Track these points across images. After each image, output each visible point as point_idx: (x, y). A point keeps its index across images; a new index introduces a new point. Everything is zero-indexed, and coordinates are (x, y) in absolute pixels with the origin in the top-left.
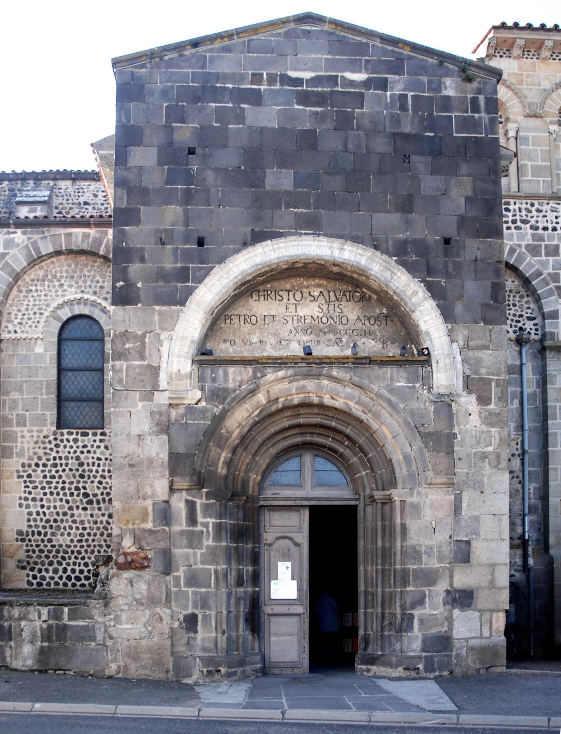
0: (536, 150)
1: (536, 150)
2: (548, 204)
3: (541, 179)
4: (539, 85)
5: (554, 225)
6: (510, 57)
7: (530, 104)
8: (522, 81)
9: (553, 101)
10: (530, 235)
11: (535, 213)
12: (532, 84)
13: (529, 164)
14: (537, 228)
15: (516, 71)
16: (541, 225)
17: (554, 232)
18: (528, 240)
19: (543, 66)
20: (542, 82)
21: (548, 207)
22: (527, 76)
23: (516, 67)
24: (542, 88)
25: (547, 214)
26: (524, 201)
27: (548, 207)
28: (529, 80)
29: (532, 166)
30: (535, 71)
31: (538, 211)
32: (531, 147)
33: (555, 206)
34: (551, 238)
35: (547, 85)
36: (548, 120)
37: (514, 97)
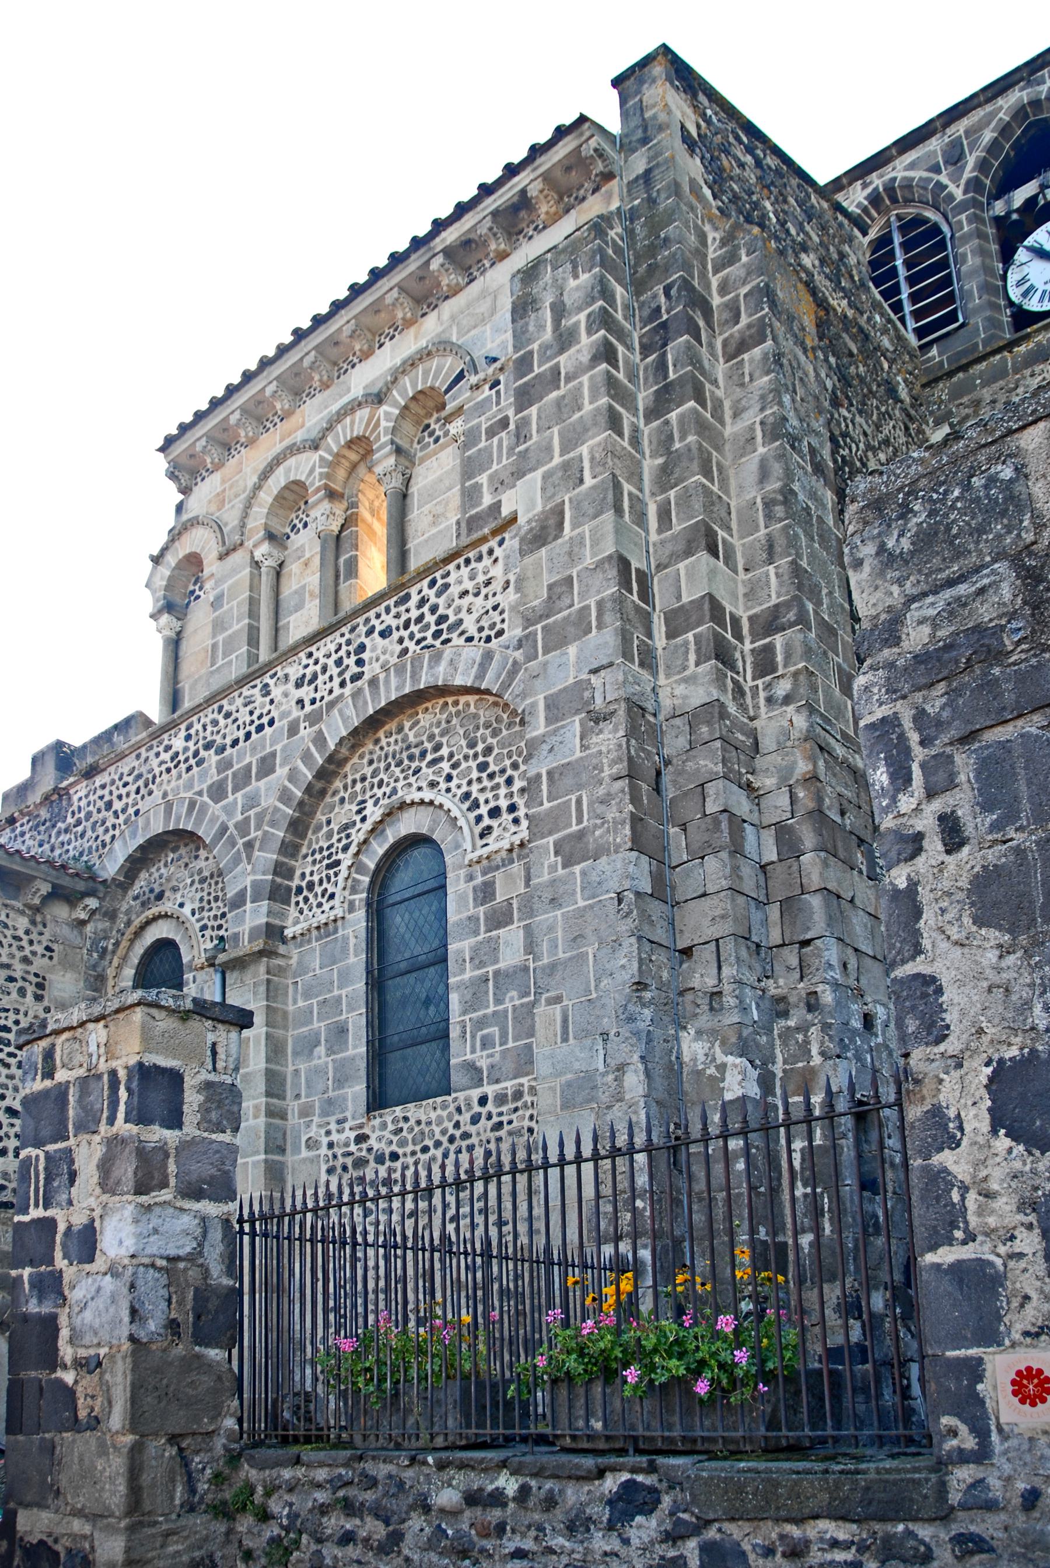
5: (248, 728)
10: (214, 765)
11: (222, 722)
14: (222, 749)
16: (228, 741)
18: (213, 777)
25: (238, 715)
26: (210, 709)
31: (228, 715)
34: (241, 756)
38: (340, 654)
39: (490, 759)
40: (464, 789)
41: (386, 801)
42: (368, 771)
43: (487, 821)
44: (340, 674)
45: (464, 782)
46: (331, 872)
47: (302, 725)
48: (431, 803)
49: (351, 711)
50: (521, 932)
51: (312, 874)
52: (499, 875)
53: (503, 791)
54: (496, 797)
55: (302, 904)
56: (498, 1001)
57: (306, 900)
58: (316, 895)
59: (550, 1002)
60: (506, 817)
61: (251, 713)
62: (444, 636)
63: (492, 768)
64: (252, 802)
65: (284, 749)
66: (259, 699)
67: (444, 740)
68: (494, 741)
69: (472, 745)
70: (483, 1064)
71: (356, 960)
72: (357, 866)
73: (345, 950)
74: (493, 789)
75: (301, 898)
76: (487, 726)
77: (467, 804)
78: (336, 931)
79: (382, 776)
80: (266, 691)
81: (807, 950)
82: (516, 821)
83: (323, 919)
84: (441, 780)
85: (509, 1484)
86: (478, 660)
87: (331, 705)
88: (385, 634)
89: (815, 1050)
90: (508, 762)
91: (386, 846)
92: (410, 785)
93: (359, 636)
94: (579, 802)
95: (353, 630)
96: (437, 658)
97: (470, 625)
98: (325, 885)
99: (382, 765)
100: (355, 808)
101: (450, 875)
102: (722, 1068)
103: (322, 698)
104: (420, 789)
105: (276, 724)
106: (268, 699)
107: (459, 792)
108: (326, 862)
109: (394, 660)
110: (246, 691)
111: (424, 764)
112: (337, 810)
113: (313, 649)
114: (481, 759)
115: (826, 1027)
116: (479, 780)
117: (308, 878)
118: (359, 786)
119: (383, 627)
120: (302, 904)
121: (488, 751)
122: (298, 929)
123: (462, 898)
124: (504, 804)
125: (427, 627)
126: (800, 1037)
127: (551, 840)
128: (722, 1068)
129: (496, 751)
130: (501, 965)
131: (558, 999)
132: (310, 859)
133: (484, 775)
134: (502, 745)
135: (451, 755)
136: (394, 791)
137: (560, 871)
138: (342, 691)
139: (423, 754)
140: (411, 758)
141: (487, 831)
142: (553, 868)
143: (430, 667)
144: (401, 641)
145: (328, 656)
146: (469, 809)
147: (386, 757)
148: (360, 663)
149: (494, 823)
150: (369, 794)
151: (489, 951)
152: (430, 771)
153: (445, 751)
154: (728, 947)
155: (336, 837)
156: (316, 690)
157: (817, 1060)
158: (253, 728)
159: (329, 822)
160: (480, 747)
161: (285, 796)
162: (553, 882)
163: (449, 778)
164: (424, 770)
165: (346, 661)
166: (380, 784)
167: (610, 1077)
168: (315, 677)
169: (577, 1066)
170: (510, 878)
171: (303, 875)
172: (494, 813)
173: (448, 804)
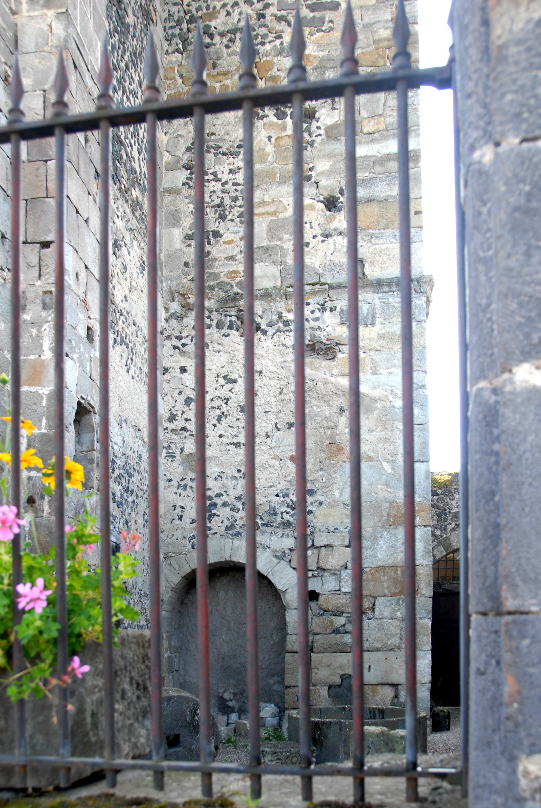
126: (34, 331)
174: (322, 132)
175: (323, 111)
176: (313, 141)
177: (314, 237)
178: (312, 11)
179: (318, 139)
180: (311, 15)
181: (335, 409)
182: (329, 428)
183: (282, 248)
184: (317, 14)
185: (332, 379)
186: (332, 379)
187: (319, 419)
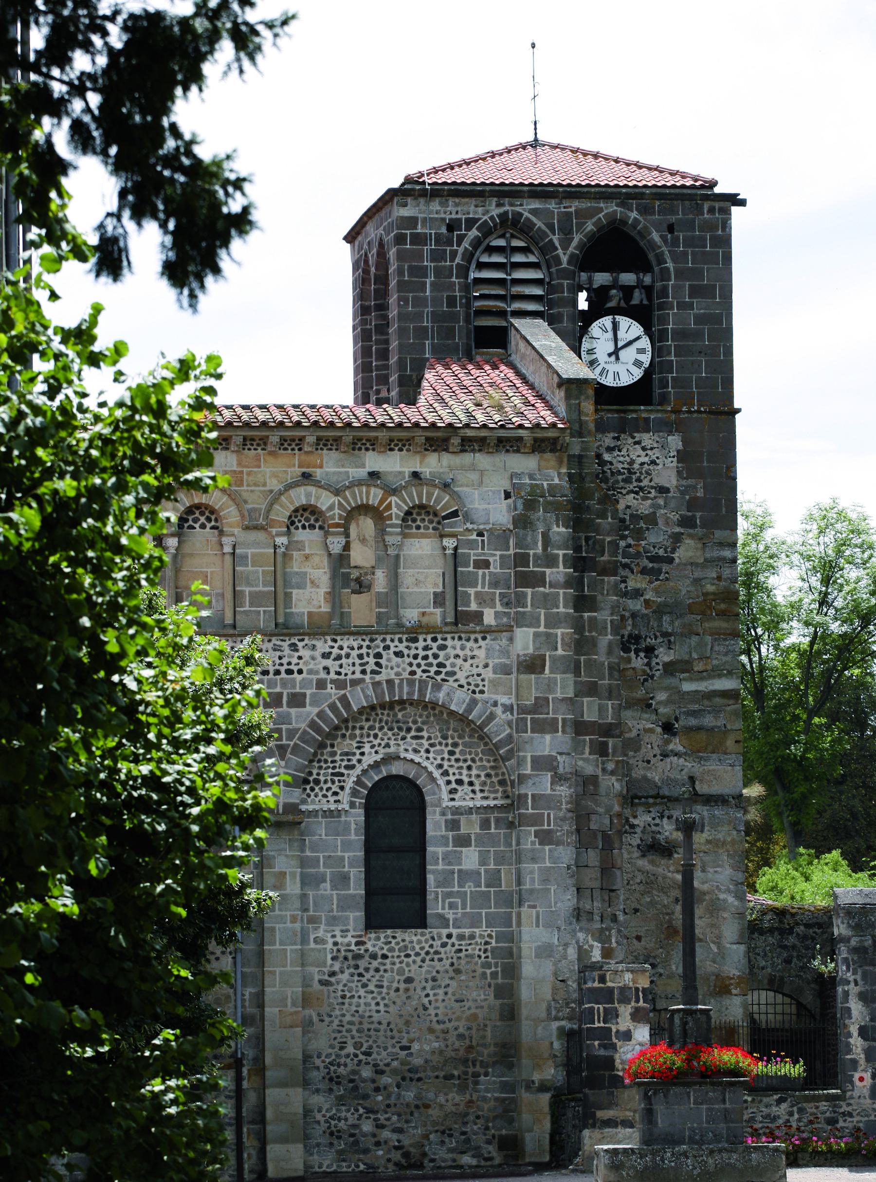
0: (257, 572)
1: (257, 572)
2: (270, 641)
3: (261, 609)
4: (265, 485)
5: (277, 667)
6: (227, 449)
7: (250, 511)
8: (242, 480)
9: (281, 506)
12: (255, 485)
13: (247, 590)
15: (235, 468)
17: (278, 677)
19: (270, 459)
20: (268, 481)
21: (270, 645)
22: (249, 474)
23: (235, 463)
24: (268, 488)
27: (270, 645)
28: (250, 478)
29: (250, 592)
30: (259, 467)
32: (250, 568)
33: (279, 643)
35: (275, 485)
36: (274, 531)
37: (231, 503)
38: (361, 651)
39: (457, 750)
40: (439, 761)
41: (382, 751)
42: (367, 725)
43: (454, 785)
44: (361, 665)
45: (439, 758)
46: (336, 779)
47: (329, 686)
48: (419, 764)
49: (370, 692)
50: (477, 854)
51: (318, 774)
52: (463, 819)
53: (465, 772)
54: (460, 774)
55: (308, 791)
56: (460, 886)
57: (312, 789)
58: (321, 789)
59: (530, 907)
60: (467, 788)
61: (280, 658)
62: (442, 676)
63: (457, 756)
64: (283, 719)
65: (312, 695)
66: (287, 651)
67: (425, 727)
68: (460, 742)
69: (445, 737)
70: (451, 917)
71: (357, 837)
72: (359, 782)
73: (346, 830)
74: (458, 768)
75: (308, 787)
76: (455, 730)
77: (440, 771)
78: (339, 816)
79: (376, 731)
80: (294, 647)
81: (612, 894)
82: (473, 792)
83: (333, 807)
84: (422, 750)
85: (749, 1099)
86: (467, 701)
87: (355, 683)
88: (399, 654)
89: (613, 940)
90: (469, 757)
91: (380, 776)
92: (399, 745)
93: (378, 647)
94: (549, 815)
95: (372, 640)
96: (437, 687)
97: (461, 676)
98: (329, 785)
99: (377, 725)
100: (355, 745)
101: (429, 809)
102: (592, 946)
103: (346, 675)
104: (406, 750)
105: (304, 675)
106: (296, 654)
107: (436, 763)
108: (330, 771)
109: (406, 675)
110: (275, 640)
111: (409, 736)
112: (339, 740)
113: (338, 638)
114: (450, 748)
115: (619, 931)
116: (449, 760)
117: (315, 776)
118: (358, 732)
119: (397, 650)
120: (308, 791)
121: (455, 745)
122: (311, 808)
123: (437, 824)
124: (466, 780)
125: (431, 665)
127: (533, 829)
128: (592, 946)
129: (461, 747)
130: (463, 867)
131: (534, 907)
132: (315, 764)
133: (453, 758)
134: (465, 745)
135: (429, 738)
136: (388, 746)
137: (537, 846)
138: (361, 676)
139: (409, 730)
140: (400, 729)
141: (453, 791)
142: (533, 843)
143: (432, 691)
144: (411, 665)
145: (352, 649)
146: (442, 774)
147: (381, 721)
148: (378, 664)
149: (459, 788)
150: (365, 740)
151: (451, 858)
152: (414, 742)
153: (425, 734)
154: (596, 893)
155: (338, 758)
156: (341, 666)
157: (614, 945)
158: (283, 669)
159: (332, 746)
160: (450, 741)
161: (313, 725)
162: (533, 850)
163: (428, 751)
164: (409, 739)
165: (366, 659)
166: (376, 736)
167: (561, 948)
168: (339, 658)
169: (544, 940)
170: (470, 823)
171: (310, 774)
172: (460, 782)
173: (431, 768)
174: (660, 667)
175: (661, 649)
176: (653, 675)
177: (655, 756)
178: (651, 562)
179: (658, 674)
180: (651, 565)
181: (671, 899)
182: (668, 914)
183: (628, 763)
184: (656, 565)
185: (670, 874)
186: (670, 874)
187: (659, 907)
